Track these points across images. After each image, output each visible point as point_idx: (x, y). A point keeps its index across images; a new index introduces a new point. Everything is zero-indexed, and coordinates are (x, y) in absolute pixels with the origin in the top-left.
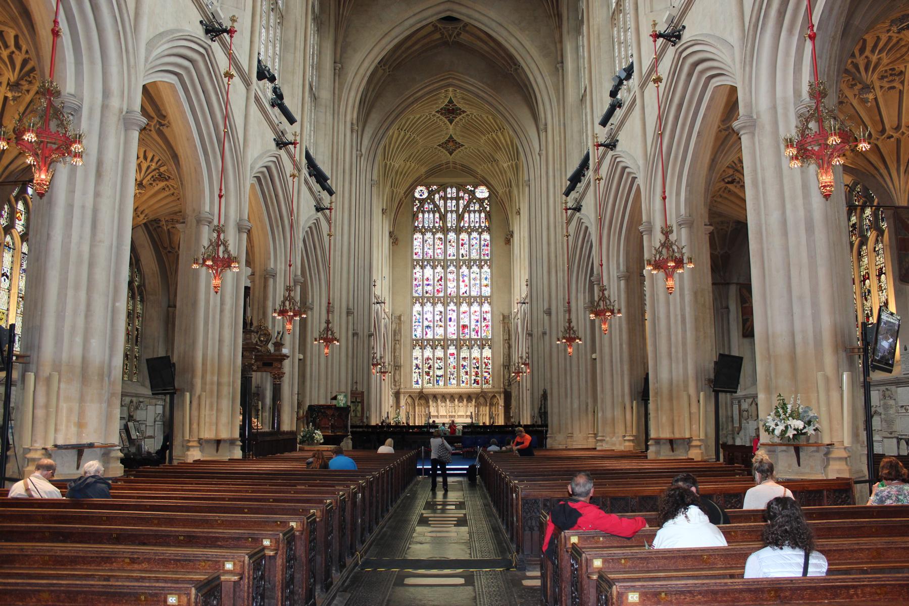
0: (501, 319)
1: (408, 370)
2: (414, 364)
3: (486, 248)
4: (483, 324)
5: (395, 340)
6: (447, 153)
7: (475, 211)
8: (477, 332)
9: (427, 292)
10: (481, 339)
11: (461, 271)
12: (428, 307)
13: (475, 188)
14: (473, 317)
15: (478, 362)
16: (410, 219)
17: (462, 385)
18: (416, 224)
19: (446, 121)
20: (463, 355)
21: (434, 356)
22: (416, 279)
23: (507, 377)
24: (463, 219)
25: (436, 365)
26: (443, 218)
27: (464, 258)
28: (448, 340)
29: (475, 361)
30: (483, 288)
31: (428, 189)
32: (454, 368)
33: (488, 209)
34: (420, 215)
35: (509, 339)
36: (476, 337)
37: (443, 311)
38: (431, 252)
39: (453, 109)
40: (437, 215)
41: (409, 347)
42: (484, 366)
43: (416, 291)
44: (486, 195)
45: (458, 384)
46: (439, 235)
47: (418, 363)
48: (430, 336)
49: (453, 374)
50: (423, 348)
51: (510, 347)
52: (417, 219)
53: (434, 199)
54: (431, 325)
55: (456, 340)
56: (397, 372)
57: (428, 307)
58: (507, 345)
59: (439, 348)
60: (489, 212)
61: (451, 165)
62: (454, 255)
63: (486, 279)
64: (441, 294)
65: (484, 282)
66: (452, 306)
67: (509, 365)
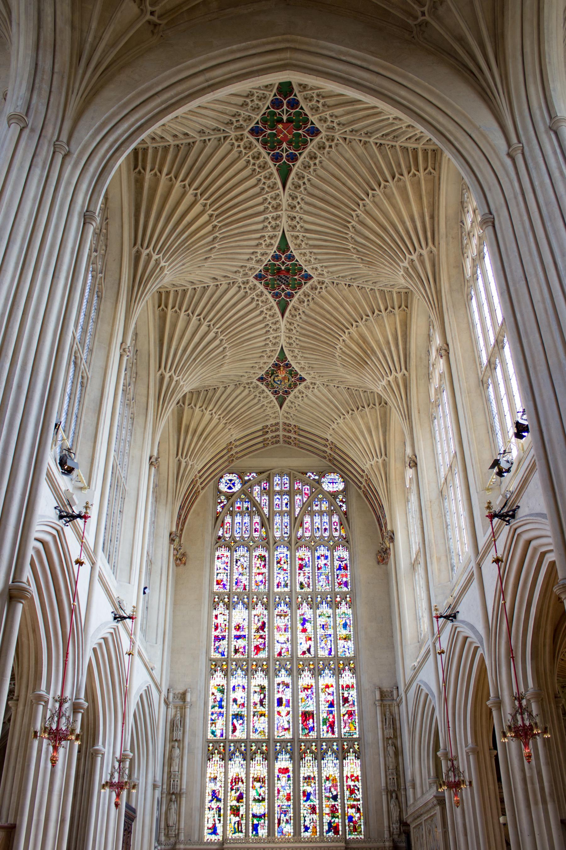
0: (378, 697)
1: (196, 803)
2: (209, 791)
3: (343, 572)
4: (343, 710)
5: (172, 740)
6: (272, 397)
7: (321, 513)
8: (332, 725)
9: (236, 651)
10: (341, 740)
11: (299, 612)
12: (239, 679)
13: (322, 474)
14: (322, 697)
15: (335, 786)
16: (210, 523)
17: (307, 834)
18: (220, 533)
19: (273, 302)
20: (305, 772)
21: (247, 774)
22: (216, 628)
23: (395, 815)
24: (301, 525)
25: (253, 794)
26: (266, 523)
27: (306, 589)
28: (276, 742)
29: (328, 784)
30: (341, 643)
31: (240, 477)
32: (288, 799)
33: (344, 508)
34: (228, 519)
35: (395, 737)
36: (330, 735)
37: (266, 685)
38: (244, 580)
39: (288, 270)
40: (257, 519)
41: (199, 755)
42: (347, 793)
43: (218, 648)
44: (341, 486)
45: (297, 832)
46: (260, 552)
47: (216, 788)
48: (240, 734)
49: (285, 813)
50: (227, 757)
51: (398, 753)
52: (222, 525)
53: (251, 492)
54: (244, 711)
55: (292, 741)
56: (174, 807)
57: (239, 679)
58: (391, 750)
59: (259, 757)
60: (345, 513)
61: (281, 433)
62: (286, 585)
63: (345, 626)
64: (263, 655)
65: (343, 632)
66: (284, 677)
67: (399, 789)
